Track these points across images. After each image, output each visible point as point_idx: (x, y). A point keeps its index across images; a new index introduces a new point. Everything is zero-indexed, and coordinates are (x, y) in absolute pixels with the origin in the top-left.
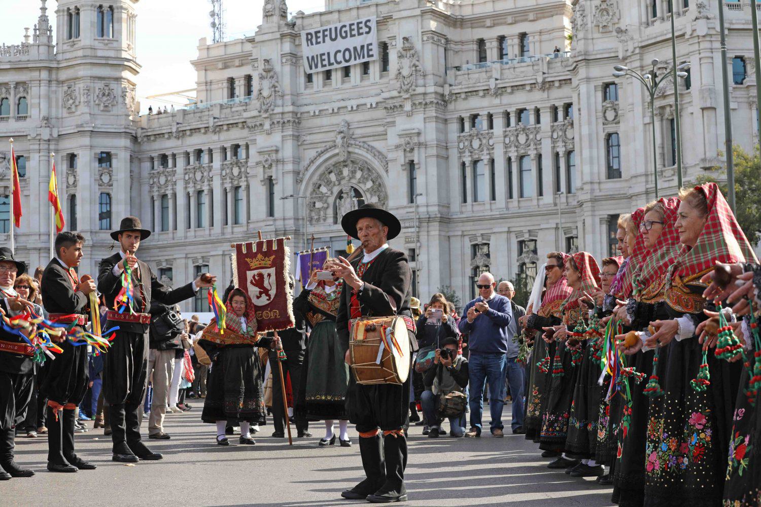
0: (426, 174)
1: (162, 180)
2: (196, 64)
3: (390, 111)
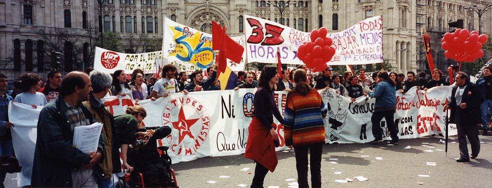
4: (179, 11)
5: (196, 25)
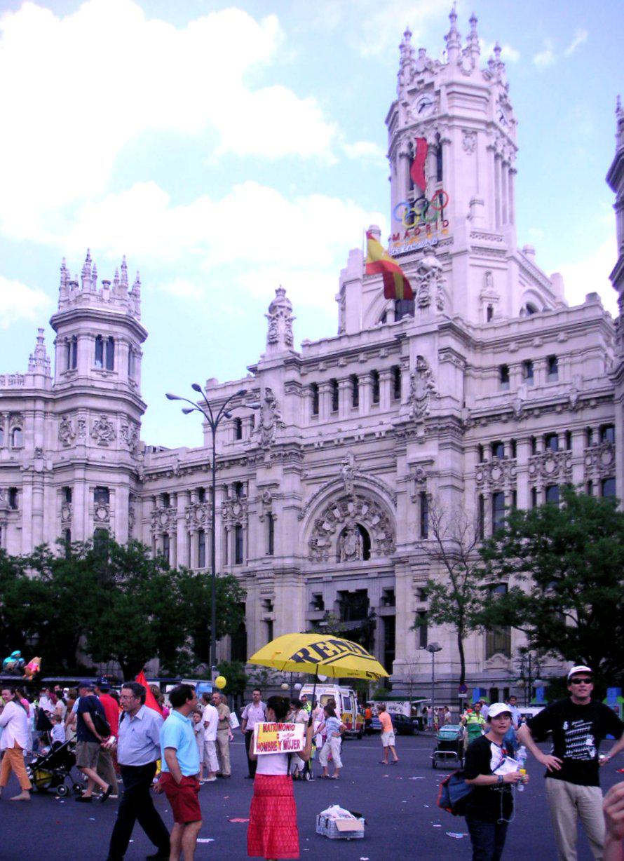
3: (401, 439)
5: (326, 532)
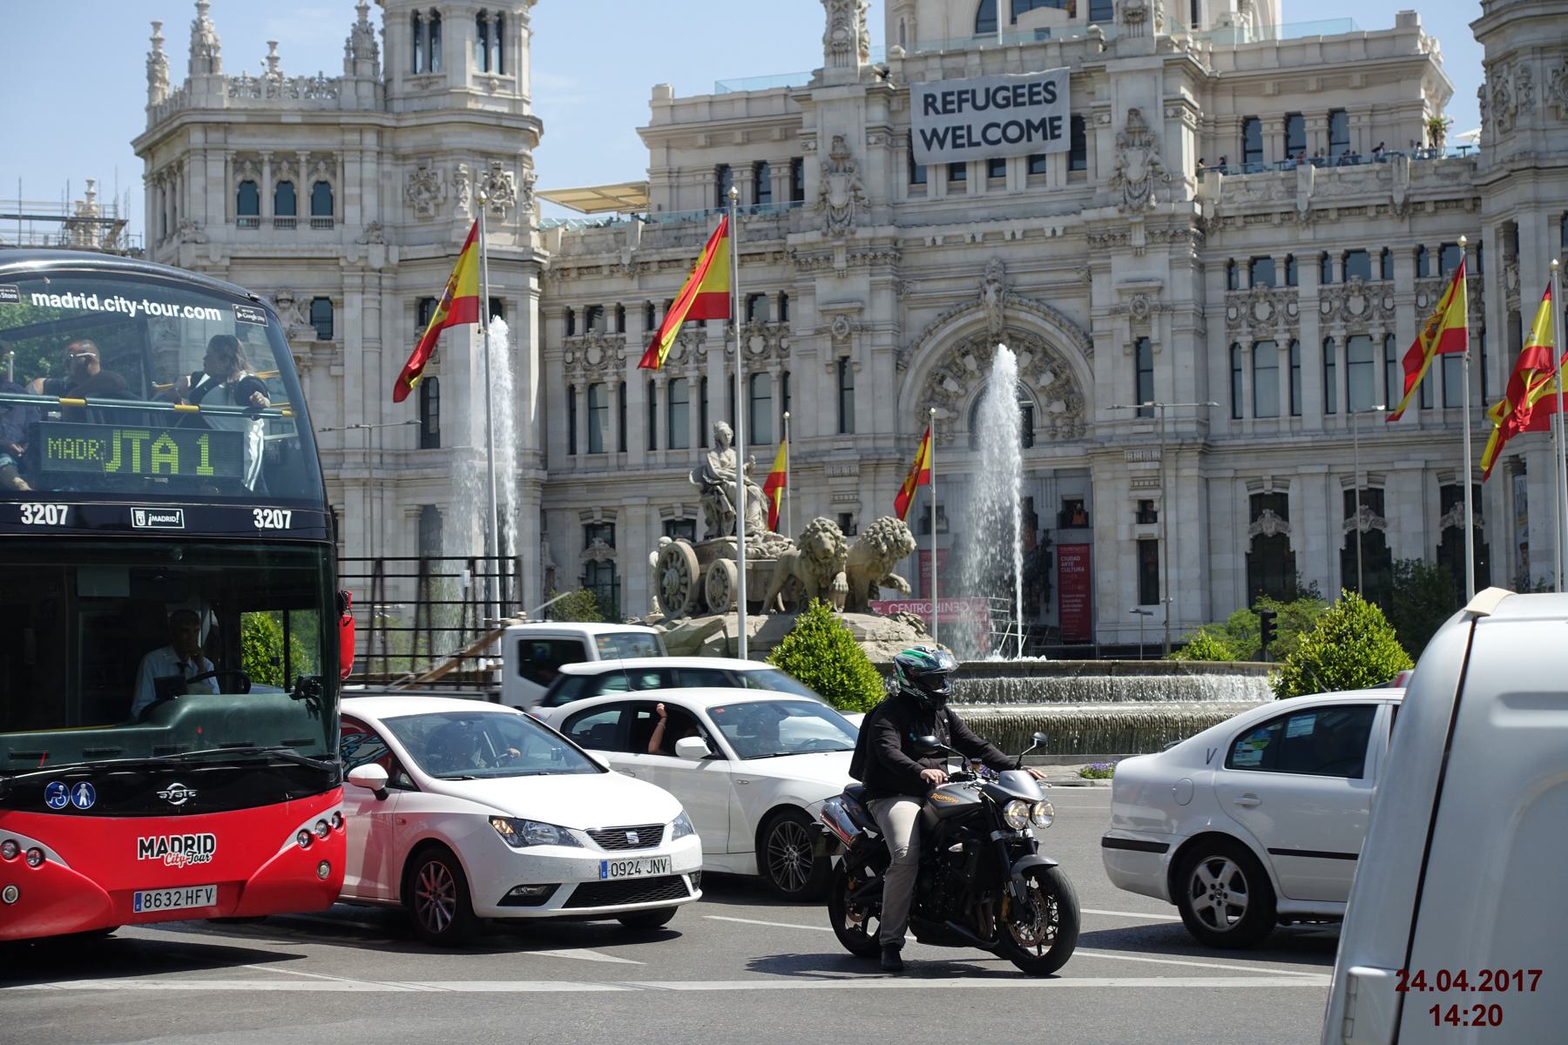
0: (1173, 364)
1: (595, 355)
2: (649, 136)
4: (866, 339)
